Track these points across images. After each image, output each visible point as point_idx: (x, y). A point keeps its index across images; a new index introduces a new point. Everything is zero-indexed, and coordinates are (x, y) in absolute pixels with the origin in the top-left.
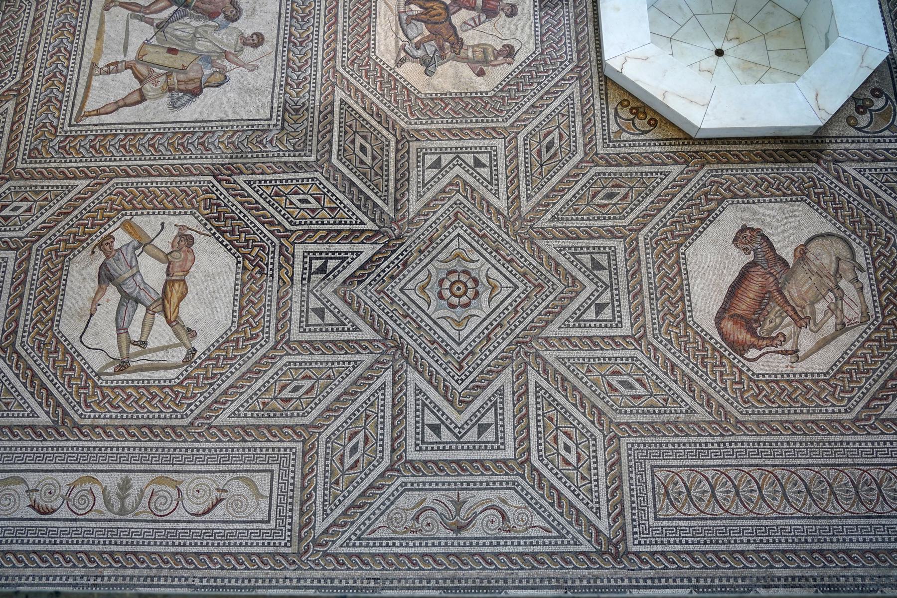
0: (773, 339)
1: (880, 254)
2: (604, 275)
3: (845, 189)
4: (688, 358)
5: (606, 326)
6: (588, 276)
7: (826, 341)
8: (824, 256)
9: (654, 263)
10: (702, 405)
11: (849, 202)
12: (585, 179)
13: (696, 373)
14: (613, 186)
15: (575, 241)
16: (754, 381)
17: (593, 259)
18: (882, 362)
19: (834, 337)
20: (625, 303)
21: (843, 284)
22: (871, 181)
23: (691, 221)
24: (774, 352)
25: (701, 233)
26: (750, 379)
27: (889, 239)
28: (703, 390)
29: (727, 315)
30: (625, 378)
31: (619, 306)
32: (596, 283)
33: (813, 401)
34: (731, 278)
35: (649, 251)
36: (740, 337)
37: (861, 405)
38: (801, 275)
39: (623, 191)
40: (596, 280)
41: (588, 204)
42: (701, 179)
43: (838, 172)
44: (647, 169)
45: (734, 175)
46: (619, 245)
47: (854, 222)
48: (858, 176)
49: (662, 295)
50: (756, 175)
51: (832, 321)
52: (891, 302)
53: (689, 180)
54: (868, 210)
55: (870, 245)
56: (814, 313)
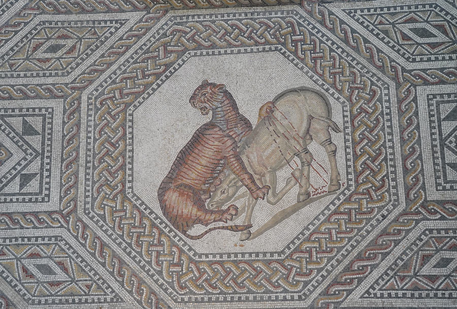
0: (224, 212)
1: (362, 110)
2: (35, 141)
3: (329, 34)
4: (122, 237)
5: (30, 200)
6: (16, 143)
7: (286, 214)
8: (293, 115)
9: (96, 126)
10: (130, 292)
11: (331, 50)
12: (27, 29)
13: (129, 254)
14: (59, 37)
15: (7, 102)
16: (196, 263)
17: (25, 122)
18: (350, 239)
19: (295, 209)
20: (56, 173)
21: (313, 147)
22: (362, 23)
23: (144, 77)
24: (223, 228)
25: (154, 90)
26: (191, 260)
27: (375, 92)
28: (134, 274)
29: (172, 186)
30: (44, 261)
31: (49, 177)
32: (25, 151)
33: (262, 285)
34: (181, 142)
35: (92, 113)
36: (185, 211)
37: (319, 290)
38: (264, 137)
39: (70, 43)
40: (25, 147)
41: (27, 58)
42: (162, 28)
43: (323, 16)
44: (100, 17)
45: (201, 22)
46: (57, 106)
47: (334, 74)
48: (345, 18)
49: (100, 163)
50: (226, 21)
51: (295, 190)
52: (369, 167)
53: (148, 29)
54: (354, 59)
55: (350, 100)
56: (274, 181)
